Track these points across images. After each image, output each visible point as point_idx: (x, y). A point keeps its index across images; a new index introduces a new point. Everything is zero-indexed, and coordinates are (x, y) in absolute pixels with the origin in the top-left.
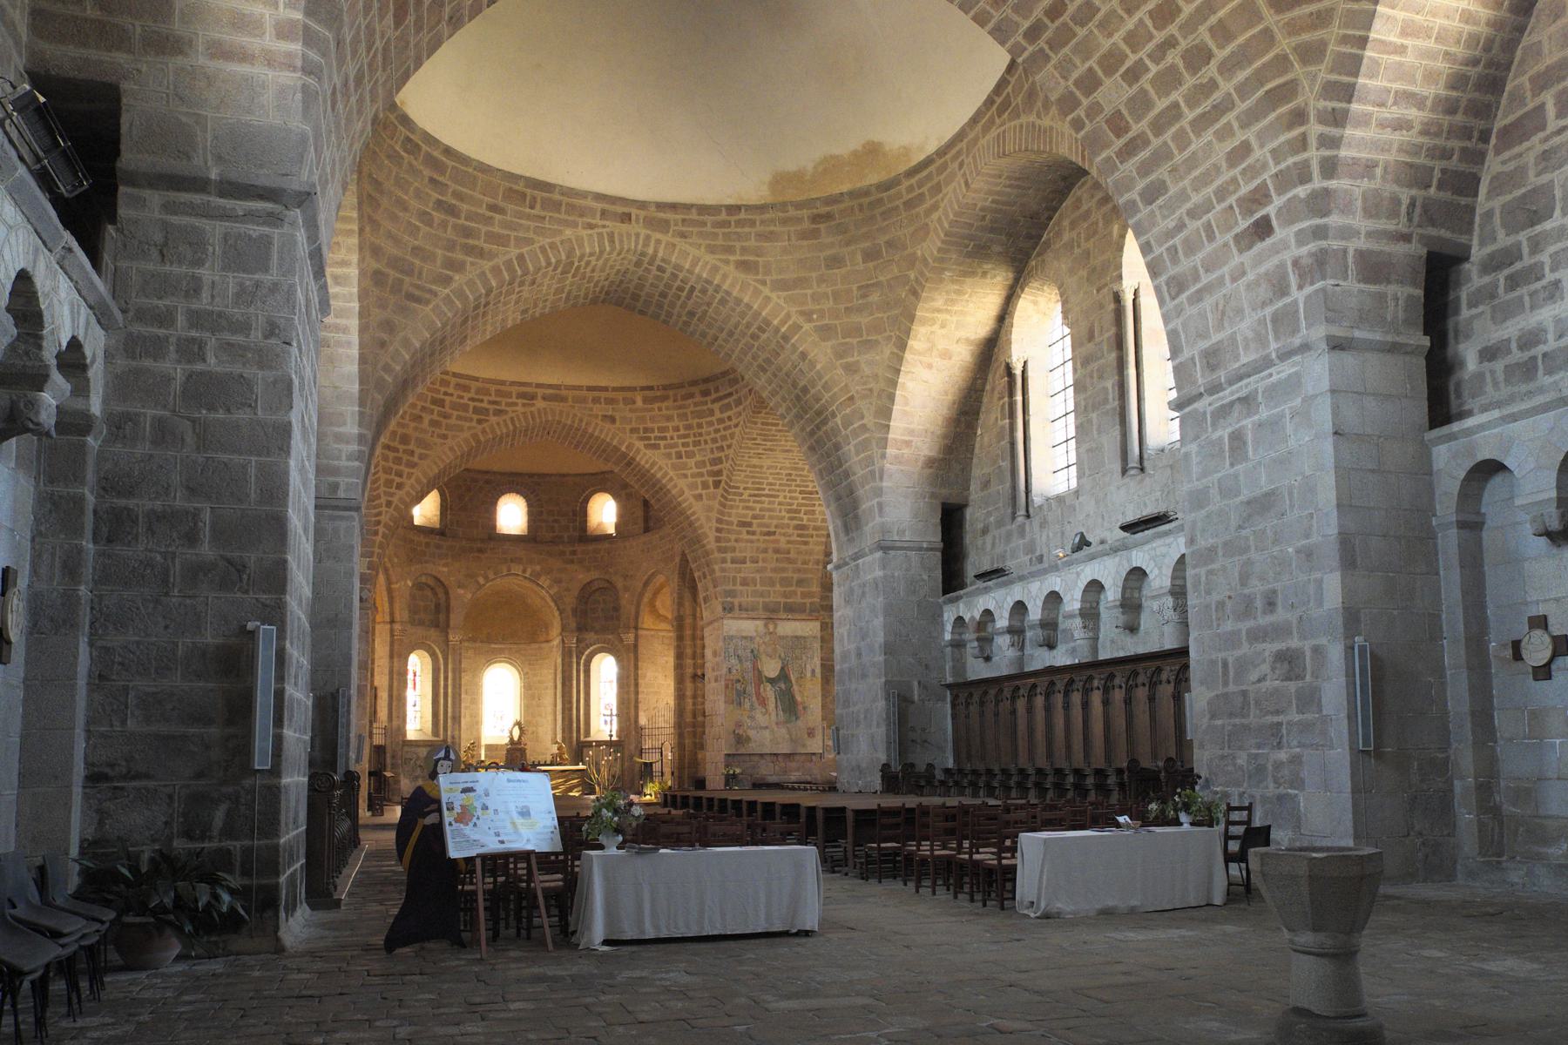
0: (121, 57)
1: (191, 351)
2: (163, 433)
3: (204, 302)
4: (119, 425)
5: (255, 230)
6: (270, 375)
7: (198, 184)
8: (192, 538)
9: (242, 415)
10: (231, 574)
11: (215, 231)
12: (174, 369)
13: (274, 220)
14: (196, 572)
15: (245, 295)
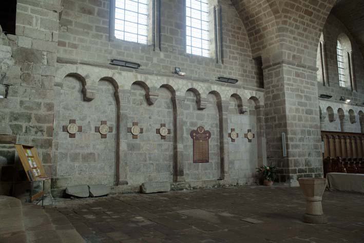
0: (260, 52)
1: (273, 92)
2: (271, 105)
3: (273, 84)
4: (266, 105)
5: (278, 70)
6: (282, 92)
7: (270, 66)
8: (275, 121)
9: (279, 100)
10: (279, 125)
11: (273, 72)
12: (271, 95)
13: (280, 67)
14: (276, 126)
15: (278, 81)
